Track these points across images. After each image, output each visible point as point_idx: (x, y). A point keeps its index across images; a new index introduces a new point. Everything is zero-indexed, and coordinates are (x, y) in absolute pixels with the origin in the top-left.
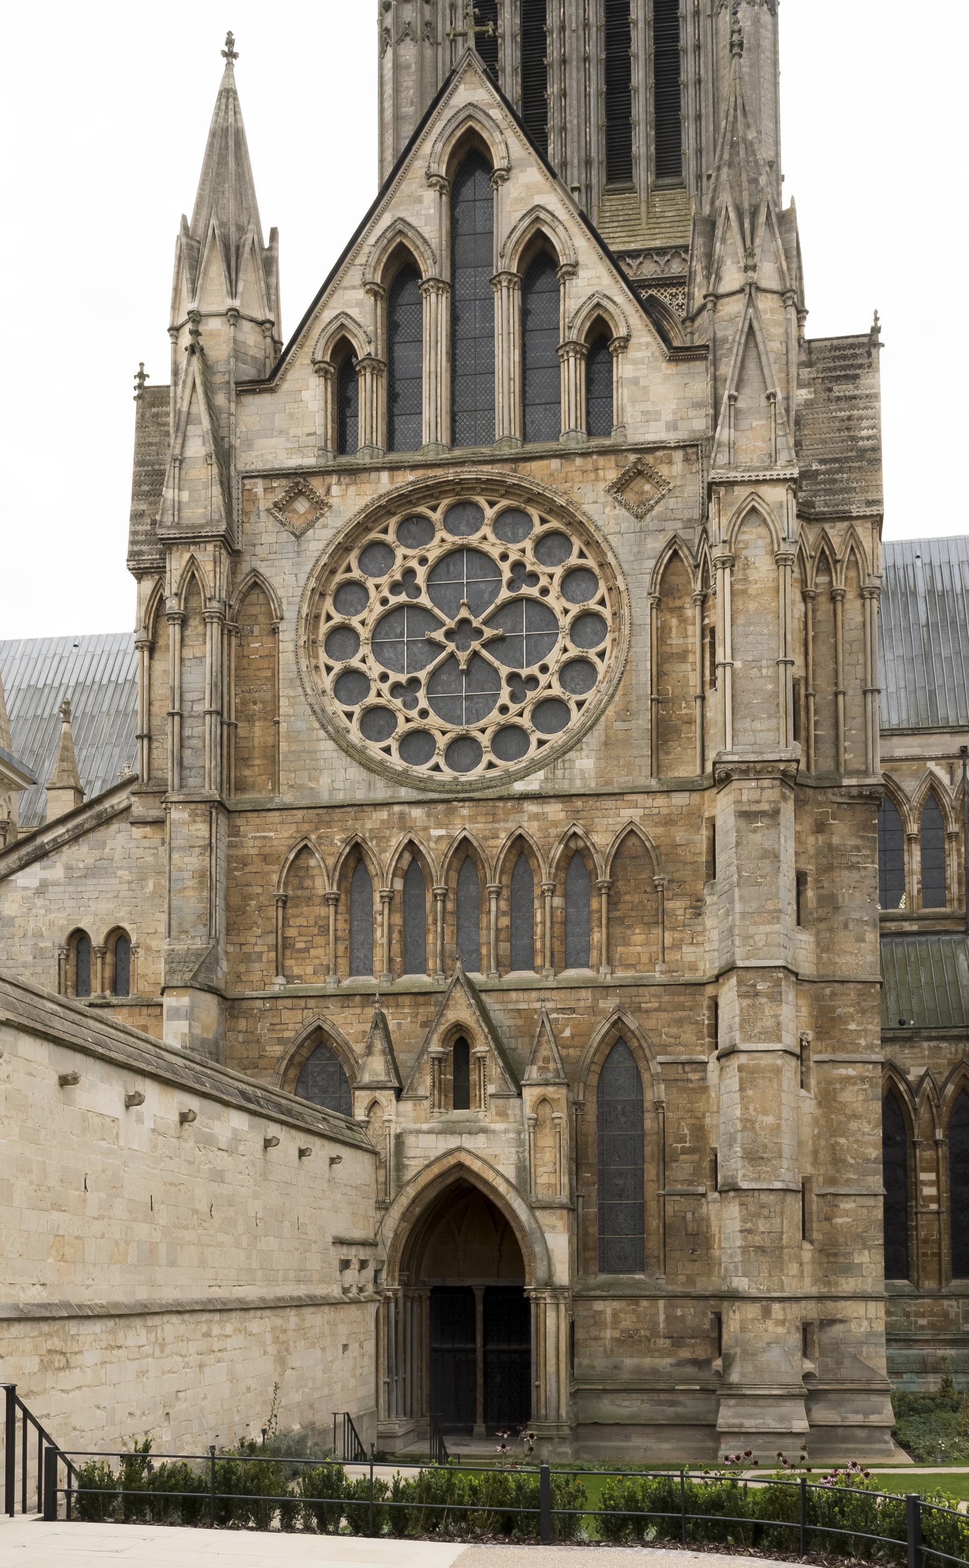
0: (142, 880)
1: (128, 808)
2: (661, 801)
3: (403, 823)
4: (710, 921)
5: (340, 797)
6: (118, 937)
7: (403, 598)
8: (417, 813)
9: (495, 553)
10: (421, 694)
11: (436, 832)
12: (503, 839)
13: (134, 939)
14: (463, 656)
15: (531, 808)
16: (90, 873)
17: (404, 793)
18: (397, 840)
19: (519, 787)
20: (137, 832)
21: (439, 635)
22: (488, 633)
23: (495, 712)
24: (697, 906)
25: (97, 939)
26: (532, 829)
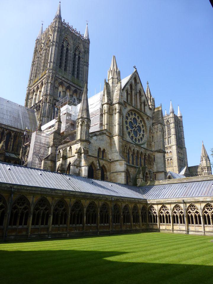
0: (107, 143)
1: (106, 133)
2: (150, 152)
3: (133, 147)
4: (155, 166)
5: (128, 141)
6: (104, 150)
7: (131, 120)
8: (134, 145)
9: (138, 120)
10: (133, 132)
11: (136, 149)
12: (141, 152)
13: (106, 152)
14: (136, 129)
15: (142, 149)
16: (102, 140)
17: (133, 143)
18: (133, 148)
19: (142, 146)
20: (107, 137)
21: (134, 126)
22: (137, 128)
23: (138, 137)
24: (153, 164)
25: (102, 150)
26: (143, 151)
